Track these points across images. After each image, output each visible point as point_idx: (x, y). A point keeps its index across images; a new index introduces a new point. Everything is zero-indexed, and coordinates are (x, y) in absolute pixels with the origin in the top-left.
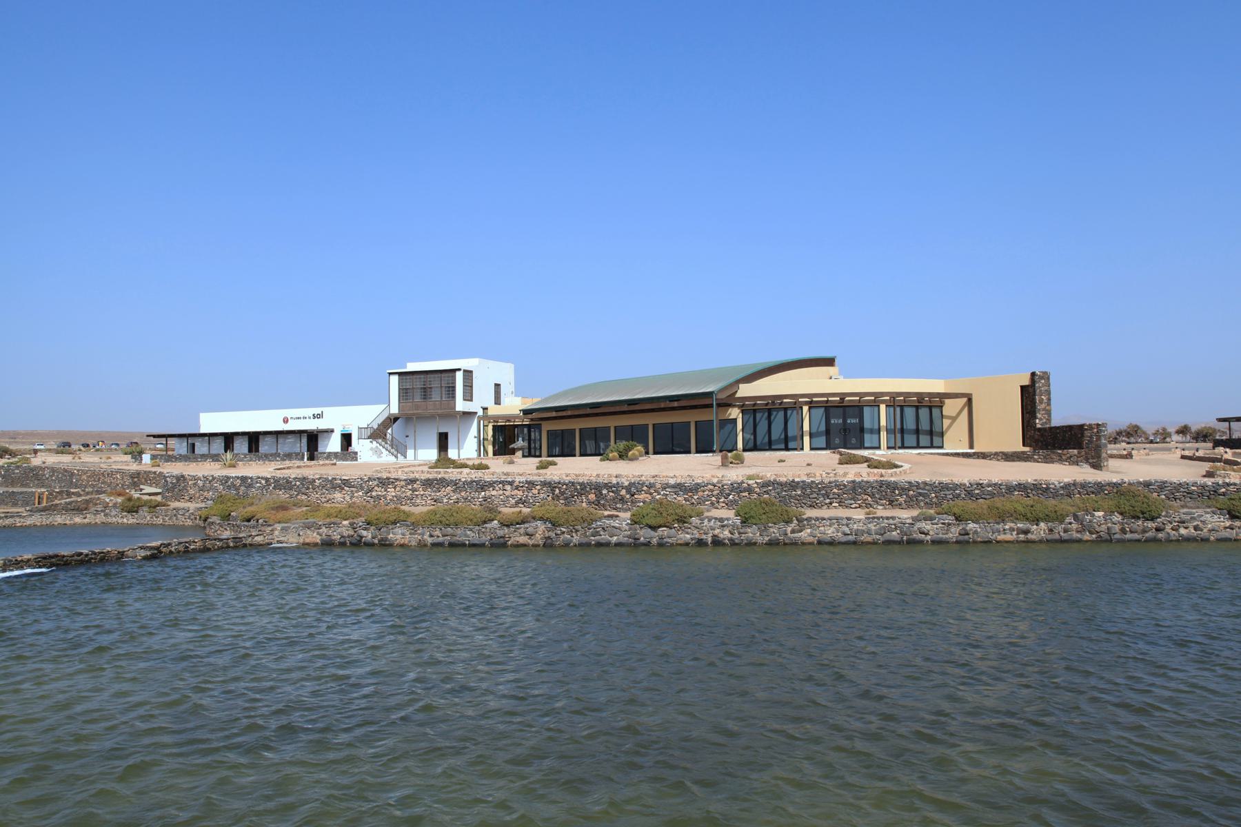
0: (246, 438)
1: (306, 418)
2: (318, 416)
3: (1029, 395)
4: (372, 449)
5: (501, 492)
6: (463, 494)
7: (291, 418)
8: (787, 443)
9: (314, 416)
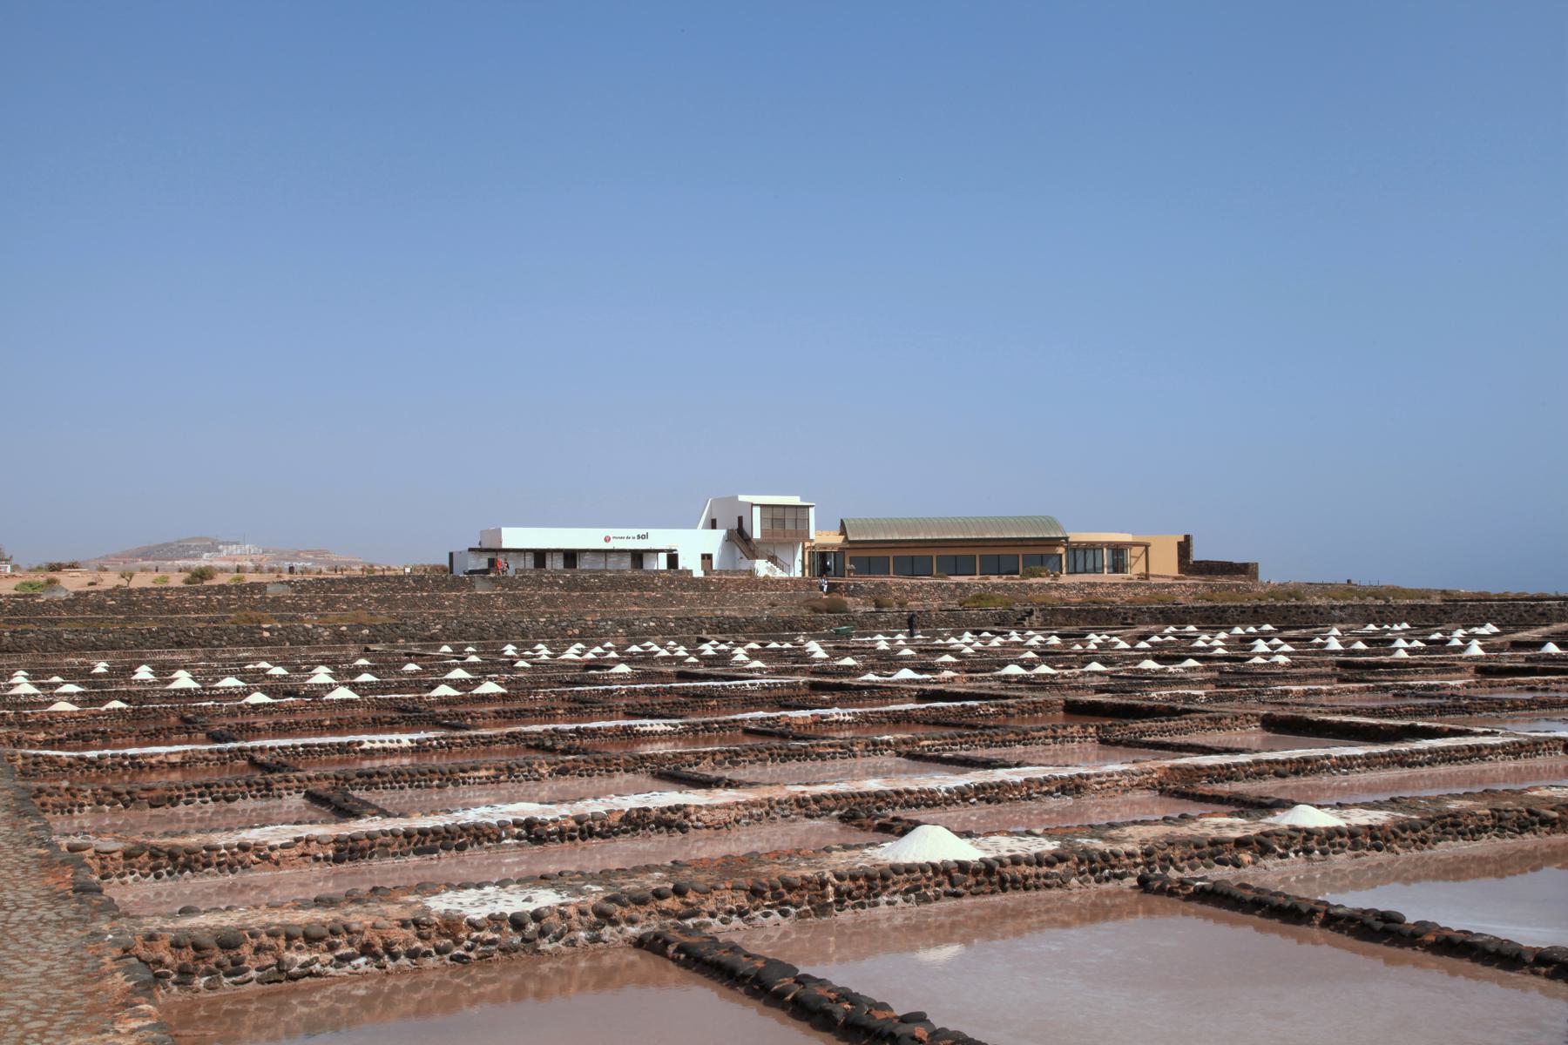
0: (562, 556)
2: (645, 537)
3: (1184, 548)
4: (767, 568)
9: (639, 537)
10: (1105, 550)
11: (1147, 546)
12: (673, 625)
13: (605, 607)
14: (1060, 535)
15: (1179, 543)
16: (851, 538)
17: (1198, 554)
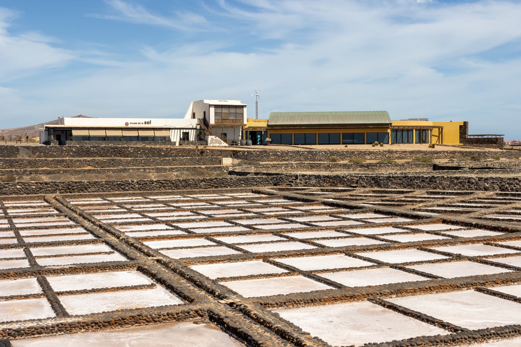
1: (140, 123)
3: (463, 128)
5: (443, 155)
6: (428, 155)
7: (131, 123)
8: (409, 141)
10: (414, 130)
11: (441, 129)
12: (34, 187)
13: (69, 167)
14: (387, 122)
15: (461, 127)
16: (269, 124)
17: (472, 131)
